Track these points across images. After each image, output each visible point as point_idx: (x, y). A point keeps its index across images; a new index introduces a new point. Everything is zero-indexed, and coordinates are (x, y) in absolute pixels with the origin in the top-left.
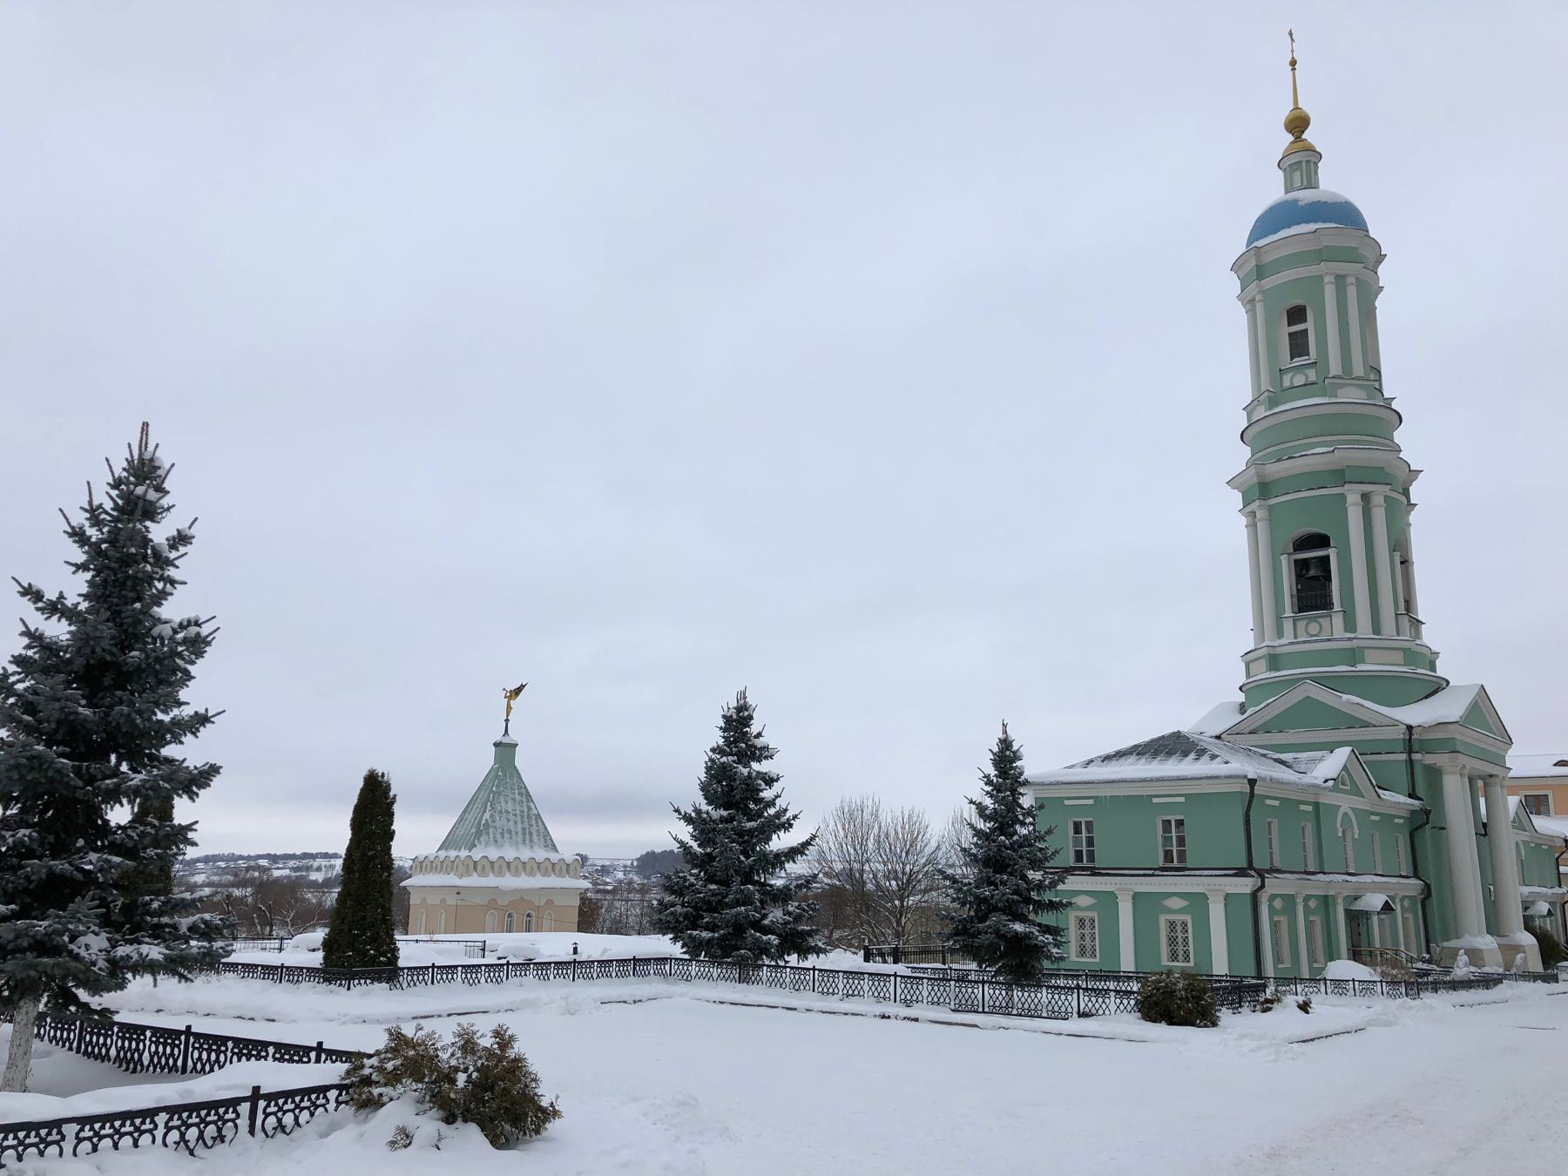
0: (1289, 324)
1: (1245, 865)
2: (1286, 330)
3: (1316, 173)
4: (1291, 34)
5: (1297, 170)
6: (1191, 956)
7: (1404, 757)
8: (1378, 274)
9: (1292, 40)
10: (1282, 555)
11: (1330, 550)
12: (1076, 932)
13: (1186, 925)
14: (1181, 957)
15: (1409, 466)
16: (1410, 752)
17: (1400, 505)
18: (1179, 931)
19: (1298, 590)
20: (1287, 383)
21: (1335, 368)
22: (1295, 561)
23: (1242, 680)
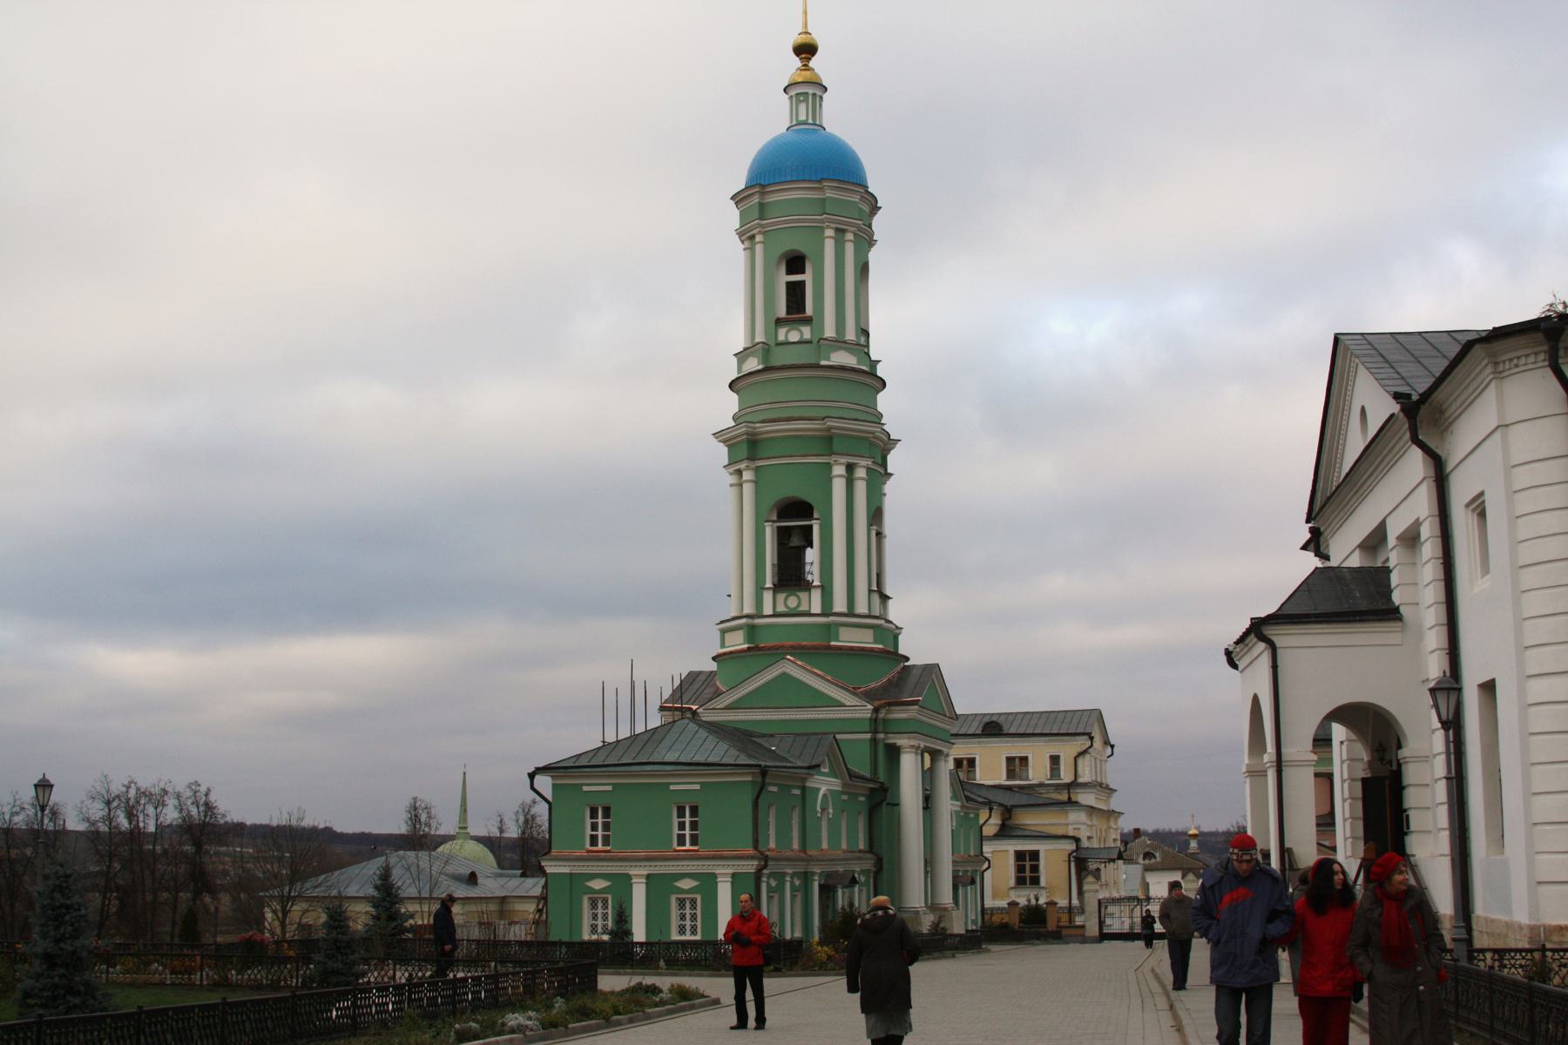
3: (821, 105)
5: (803, 101)
6: (699, 930)
8: (873, 228)
10: (766, 521)
11: (814, 522)
12: (589, 912)
13: (695, 903)
14: (688, 932)
15: (889, 436)
16: (875, 732)
17: (880, 474)
18: (599, 907)
20: (781, 338)
21: (830, 331)
22: (779, 528)
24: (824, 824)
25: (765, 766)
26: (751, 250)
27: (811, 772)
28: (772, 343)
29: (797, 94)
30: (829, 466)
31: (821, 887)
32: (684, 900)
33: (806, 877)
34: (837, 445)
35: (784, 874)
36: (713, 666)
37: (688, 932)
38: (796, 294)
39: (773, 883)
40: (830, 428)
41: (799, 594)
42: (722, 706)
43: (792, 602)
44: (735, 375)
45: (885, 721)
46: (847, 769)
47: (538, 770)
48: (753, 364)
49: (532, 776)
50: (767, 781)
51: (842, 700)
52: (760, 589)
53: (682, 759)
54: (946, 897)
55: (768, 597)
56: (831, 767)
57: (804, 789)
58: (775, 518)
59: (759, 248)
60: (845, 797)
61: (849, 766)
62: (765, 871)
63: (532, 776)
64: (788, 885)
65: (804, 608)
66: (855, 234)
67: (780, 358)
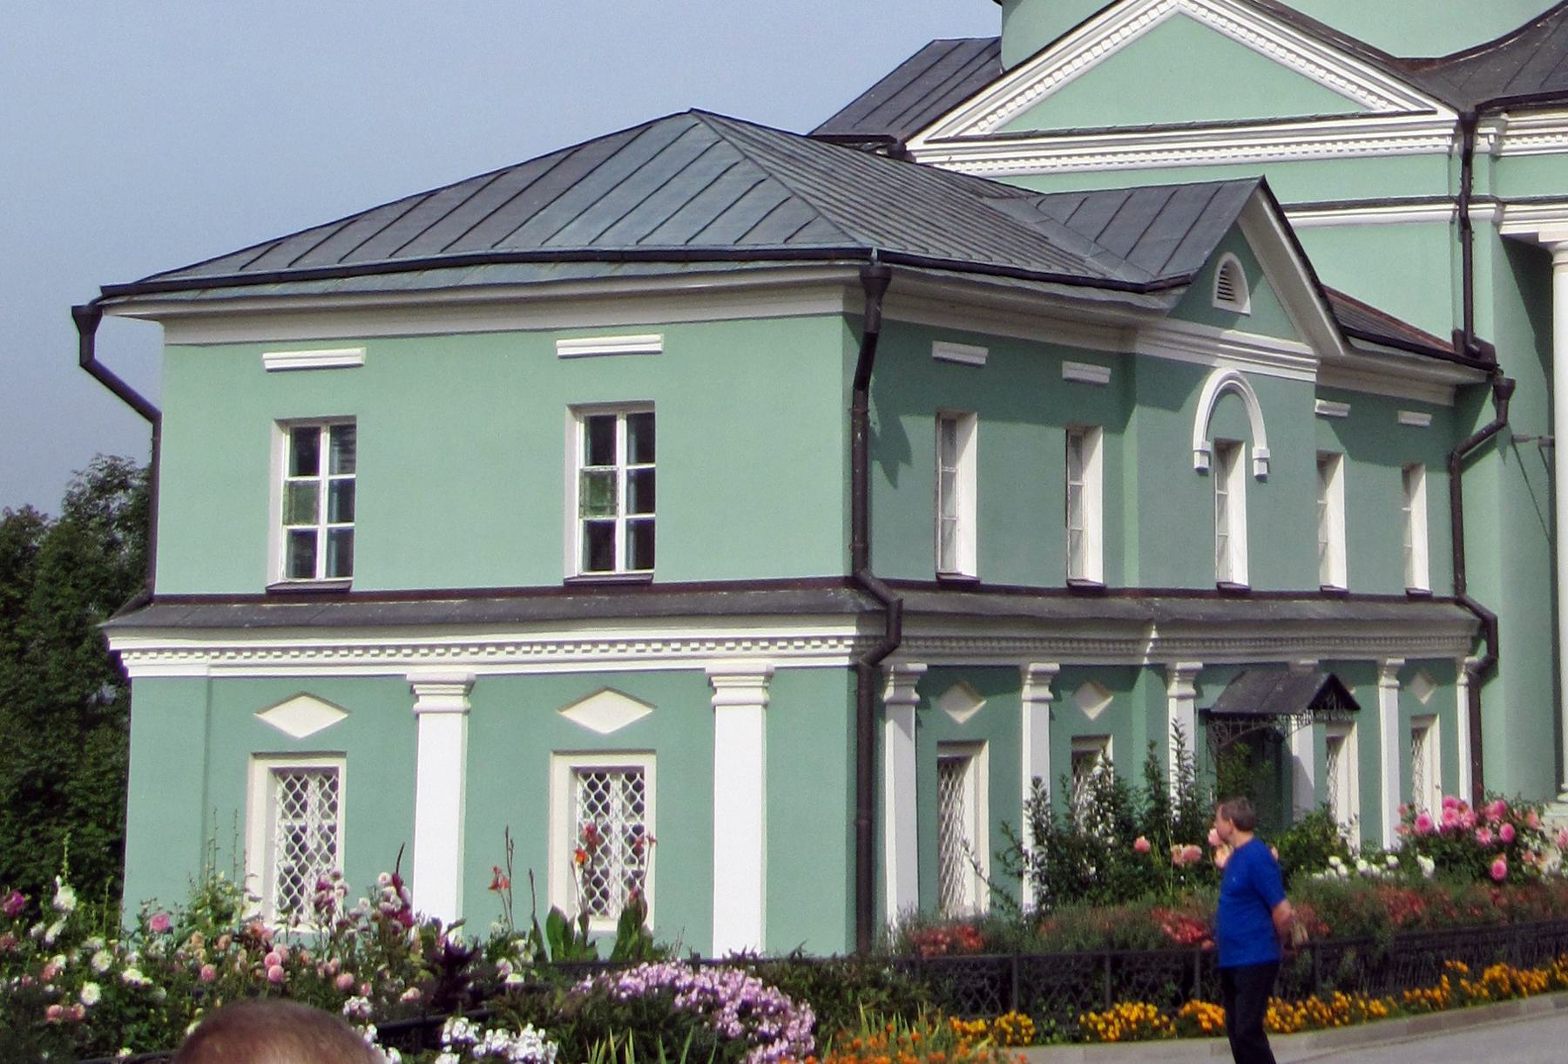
7: (1446, 211)
25: (884, 256)
32: (600, 777)
46: (1321, 291)
49: (87, 320)
51: (1370, 100)
61: (1323, 280)
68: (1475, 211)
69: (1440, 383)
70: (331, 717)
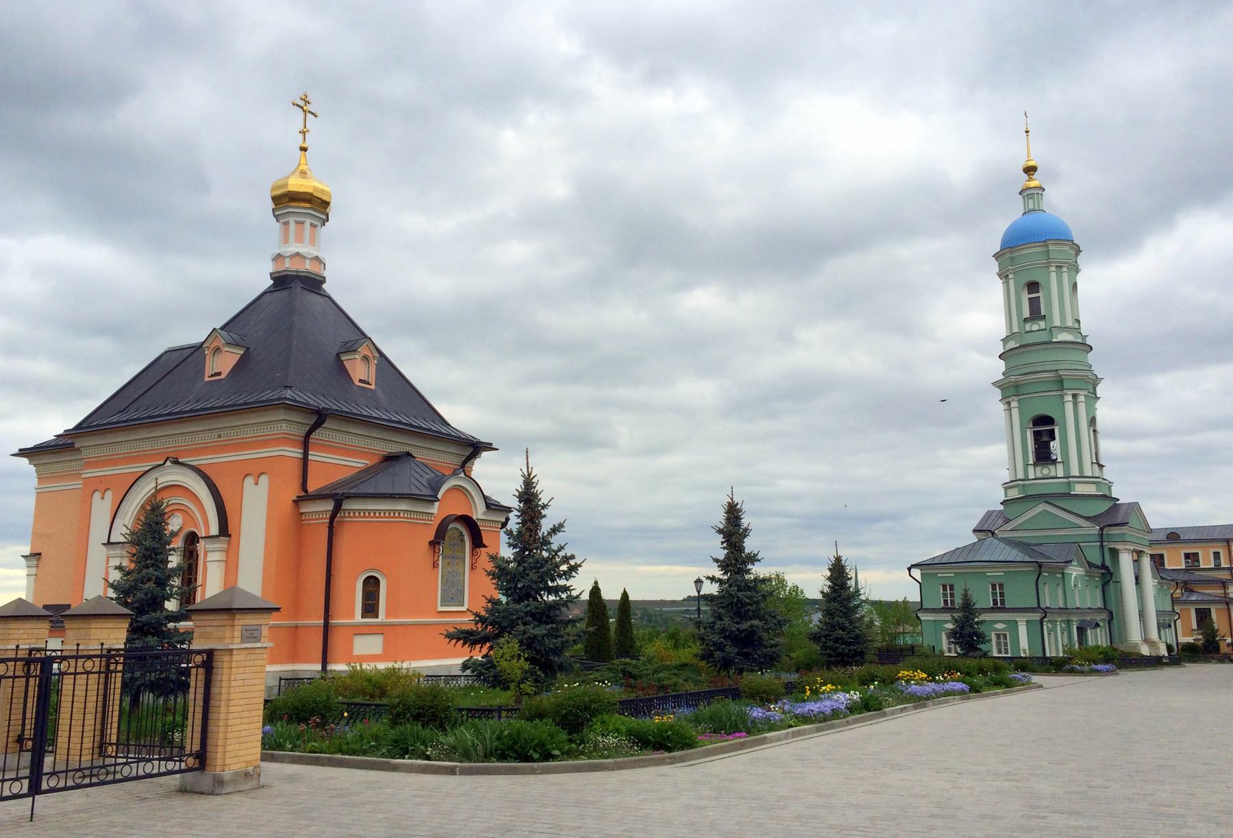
0: (1029, 294)
1: (1036, 606)
2: (1025, 297)
4: (1025, 114)
7: (1099, 544)
9: (1026, 117)
14: (1003, 652)
19: (1035, 448)
22: (1034, 431)
23: (1003, 498)
24: (1076, 592)
26: (1006, 283)
27: (1067, 564)
28: (1023, 332)
29: (1027, 195)
30: (1062, 396)
31: (1077, 627)
33: (1068, 622)
34: (1066, 385)
35: (1056, 621)
36: (1002, 507)
37: (1003, 652)
38: (1034, 304)
39: (1050, 626)
40: (1061, 376)
41: (1049, 467)
42: (1008, 529)
43: (1045, 471)
44: (1002, 351)
45: (1108, 535)
47: (913, 566)
48: (1012, 344)
49: (909, 569)
50: (1042, 570)
52: (1026, 465)
53: (992, 559)
54: (1154, 635)
55: (1031, 469)
56: (1079, 562)
57: (1063, 574)
58: (1032, 426)
59: (1012, 282)
60: (1087, 578)
62: (1045, 619)
63: (909, 569)
64: (1059, 627)
65: (1053, 474)
66: (1068, 268)
67: (1030, 339)
68: (1104, 544)
69: (1098, 573)
70: (1005, 626)
